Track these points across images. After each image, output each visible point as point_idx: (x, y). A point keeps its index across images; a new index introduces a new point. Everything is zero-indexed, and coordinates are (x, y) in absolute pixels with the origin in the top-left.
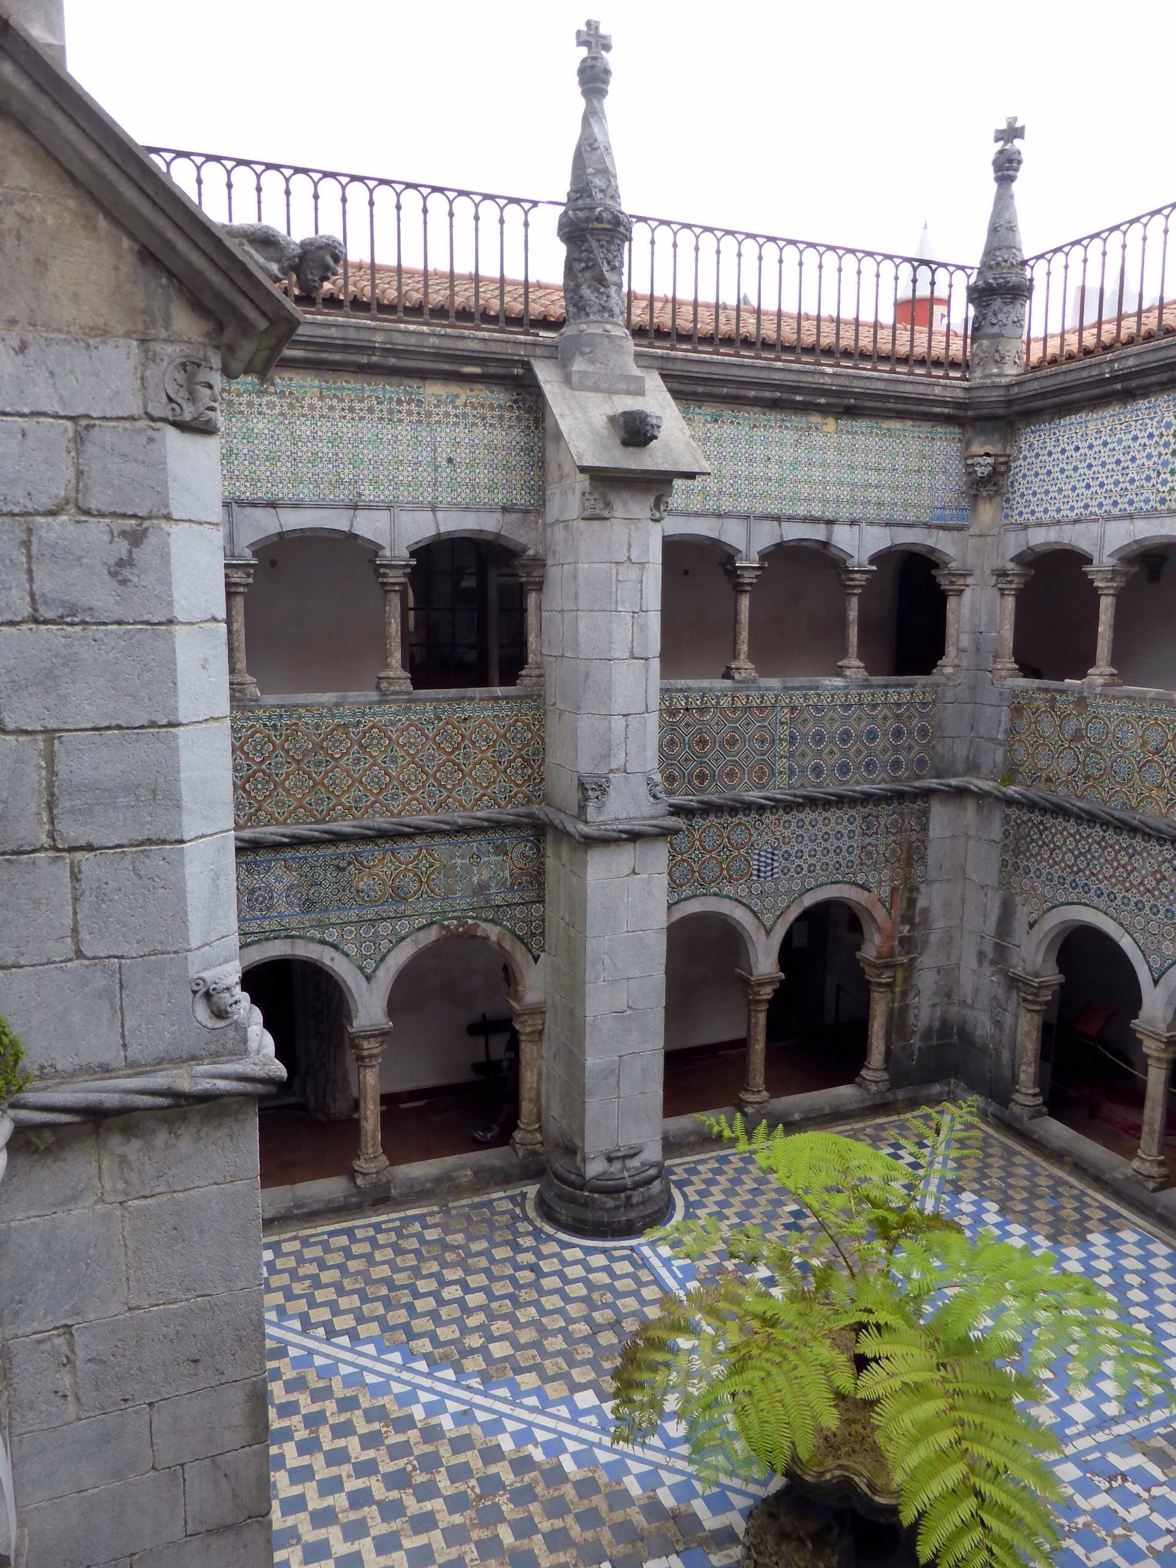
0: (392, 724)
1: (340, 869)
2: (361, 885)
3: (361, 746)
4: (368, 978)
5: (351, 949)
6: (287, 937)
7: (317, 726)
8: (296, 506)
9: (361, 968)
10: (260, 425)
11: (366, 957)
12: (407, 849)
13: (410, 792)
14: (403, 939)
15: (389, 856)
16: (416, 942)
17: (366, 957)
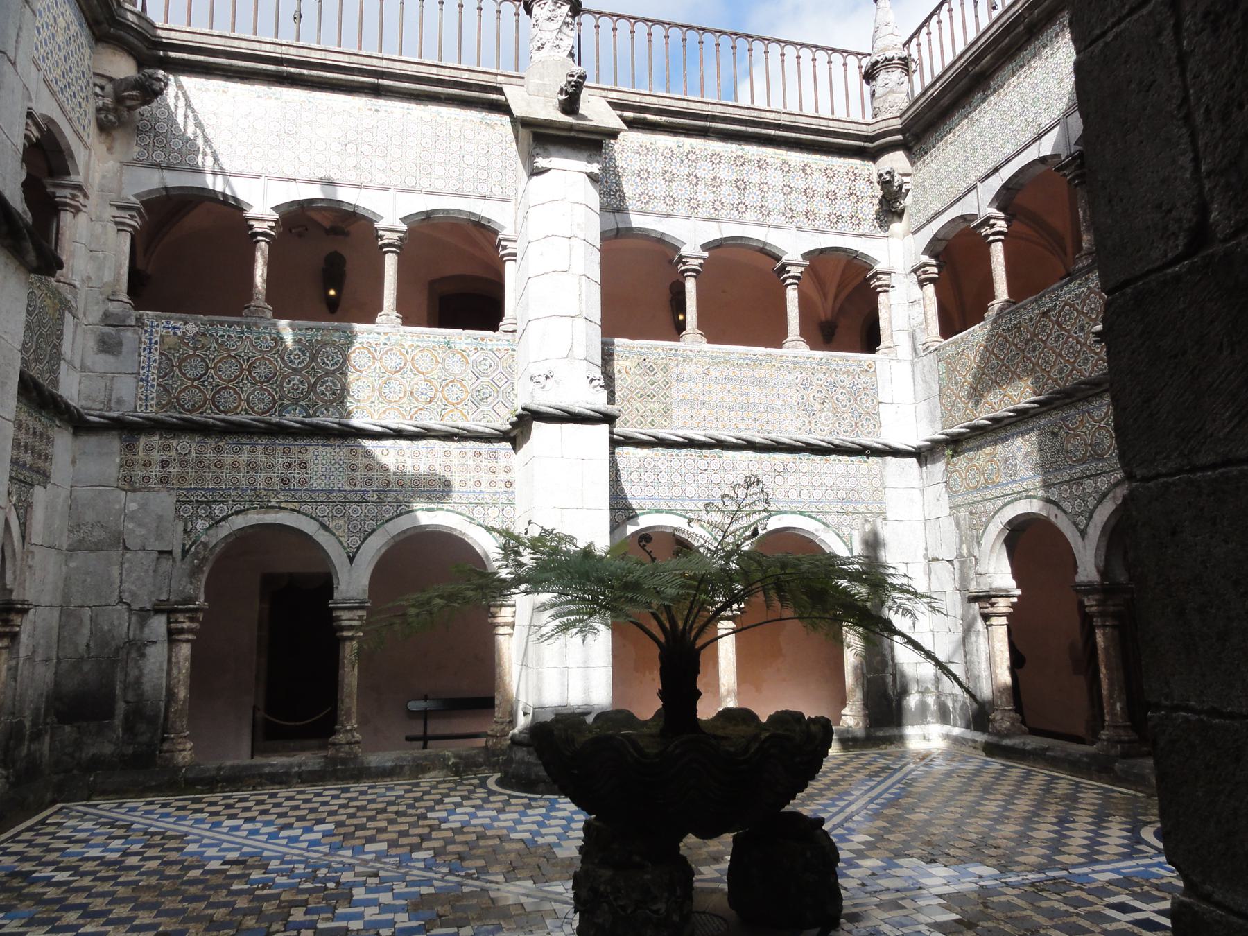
0: (1078, 297)
1: (1055, 435)
2: (1069, 447)
3: (1059, 325)
4: (1083, 533)
5: (1066, 505)
6: (1027, 497)
7: (1031, 319)
8: (1008, 161)
9: (1076, 525)
10: (986, 120)
11: (1079, 514)
12: (1098, 408)
13: (1096, 353)
14: (1104, 495)
15: (1087, 418)
16: (1114, 498)
17: (1079, 514)
